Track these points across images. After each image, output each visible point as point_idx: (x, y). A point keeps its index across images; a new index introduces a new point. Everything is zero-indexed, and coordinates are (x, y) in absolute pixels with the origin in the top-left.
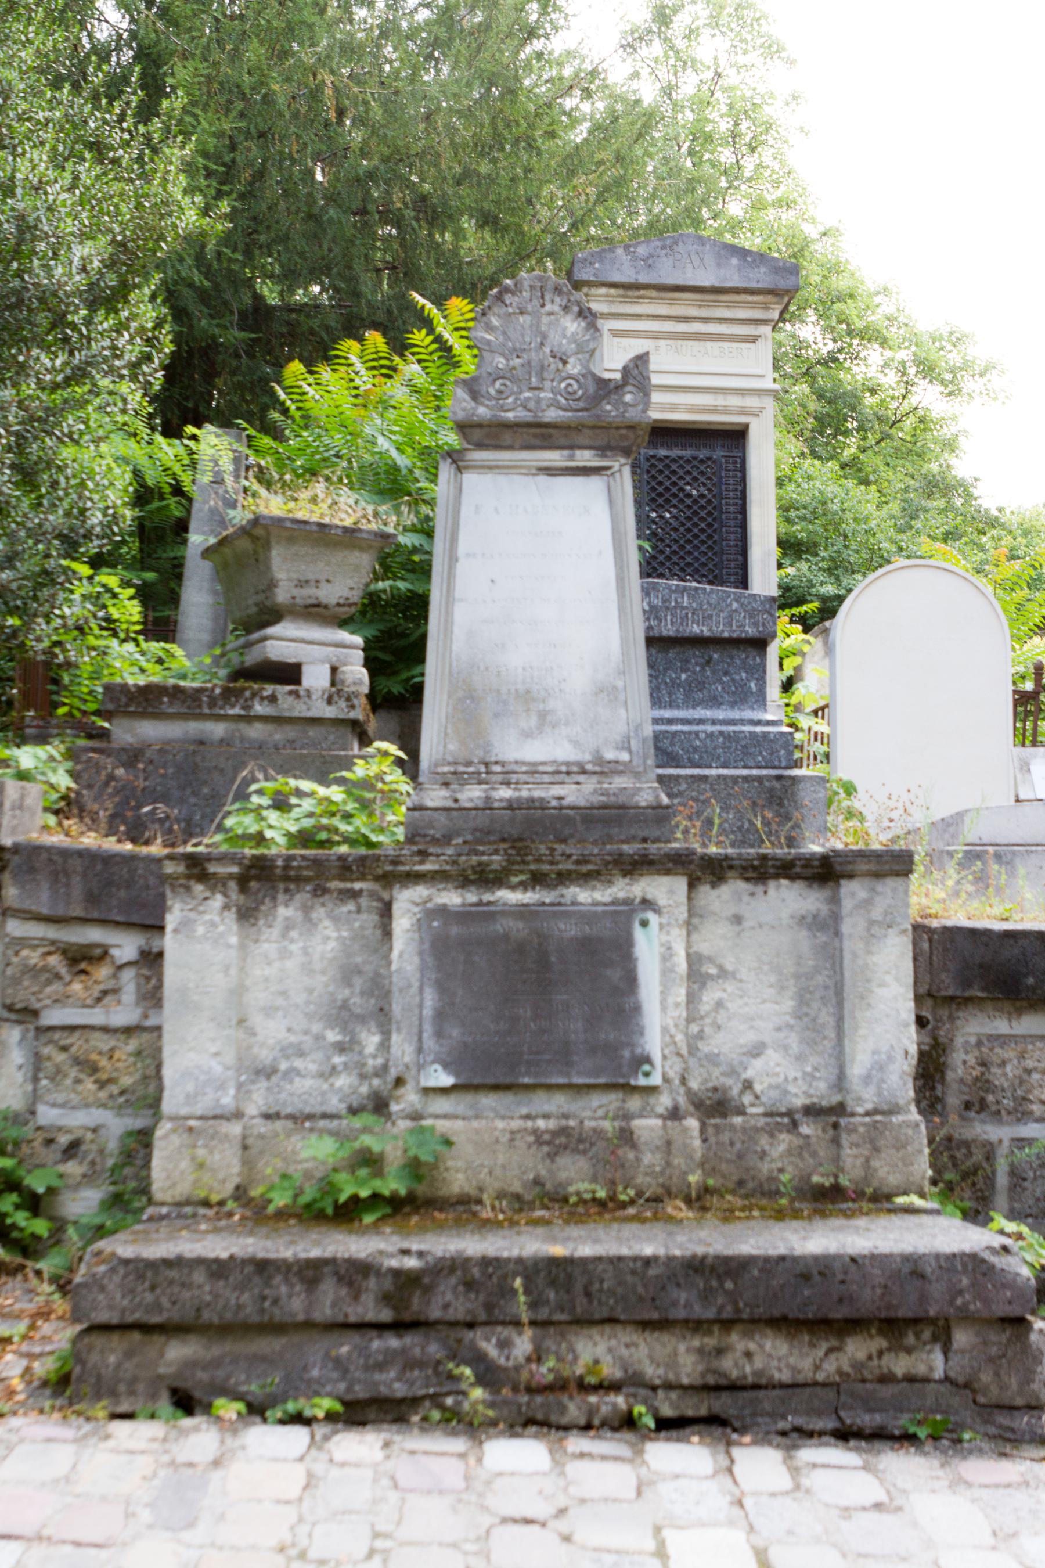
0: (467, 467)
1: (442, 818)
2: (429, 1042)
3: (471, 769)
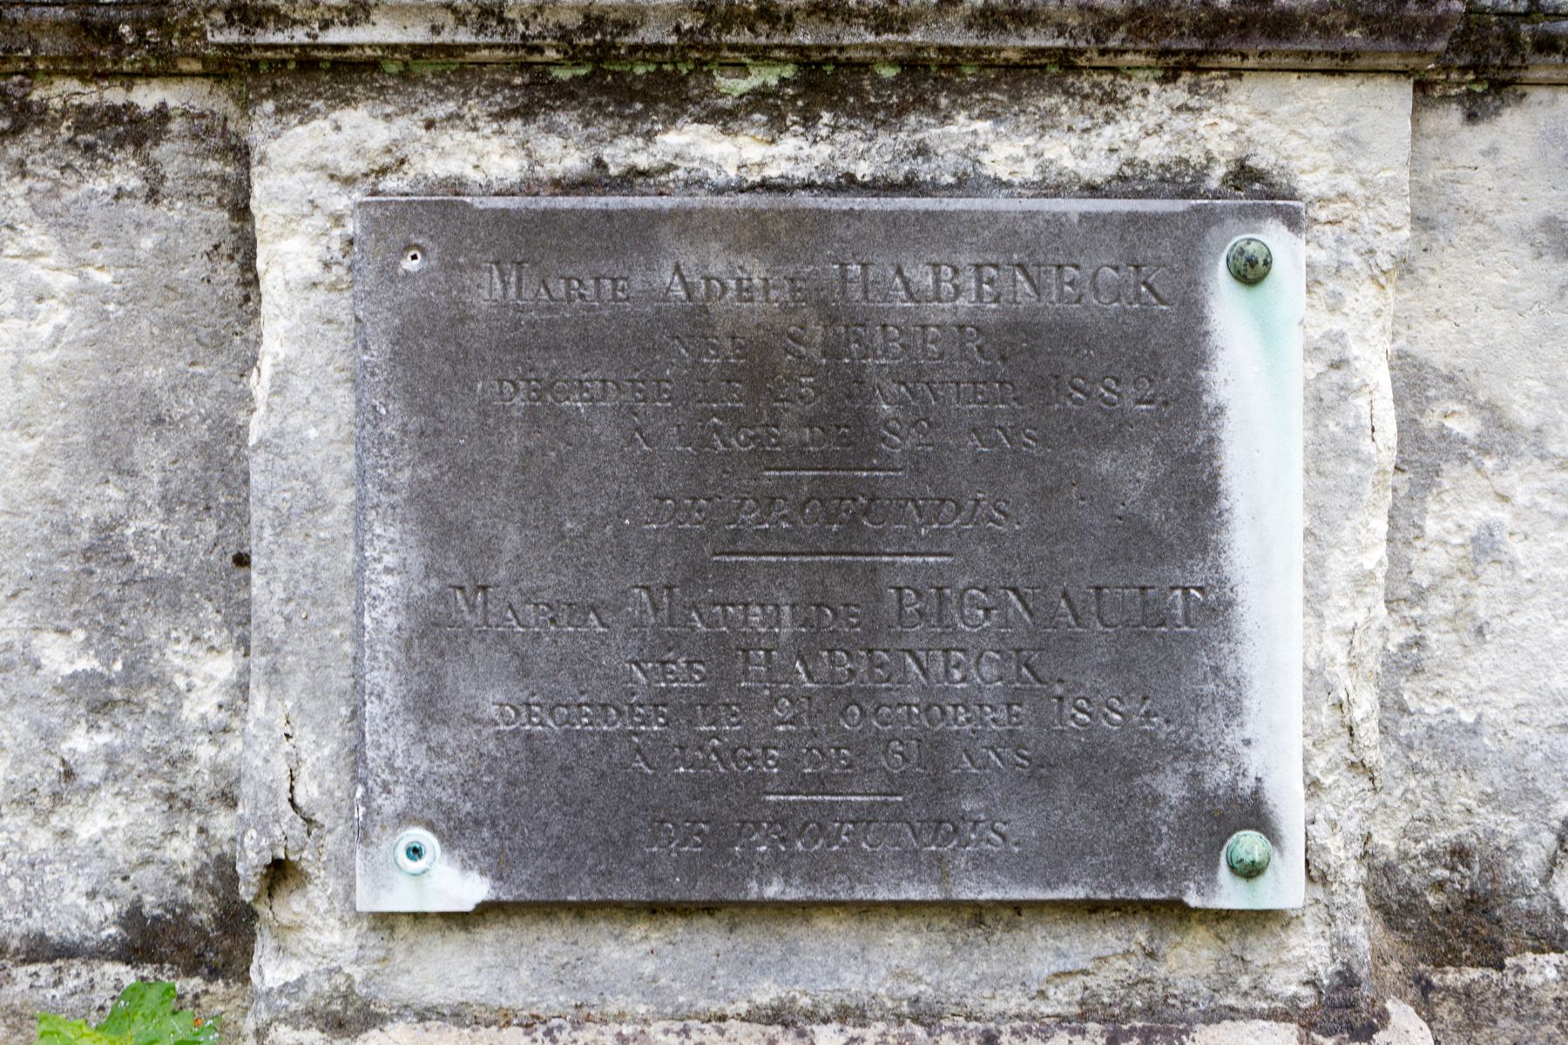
2: (391, 739)
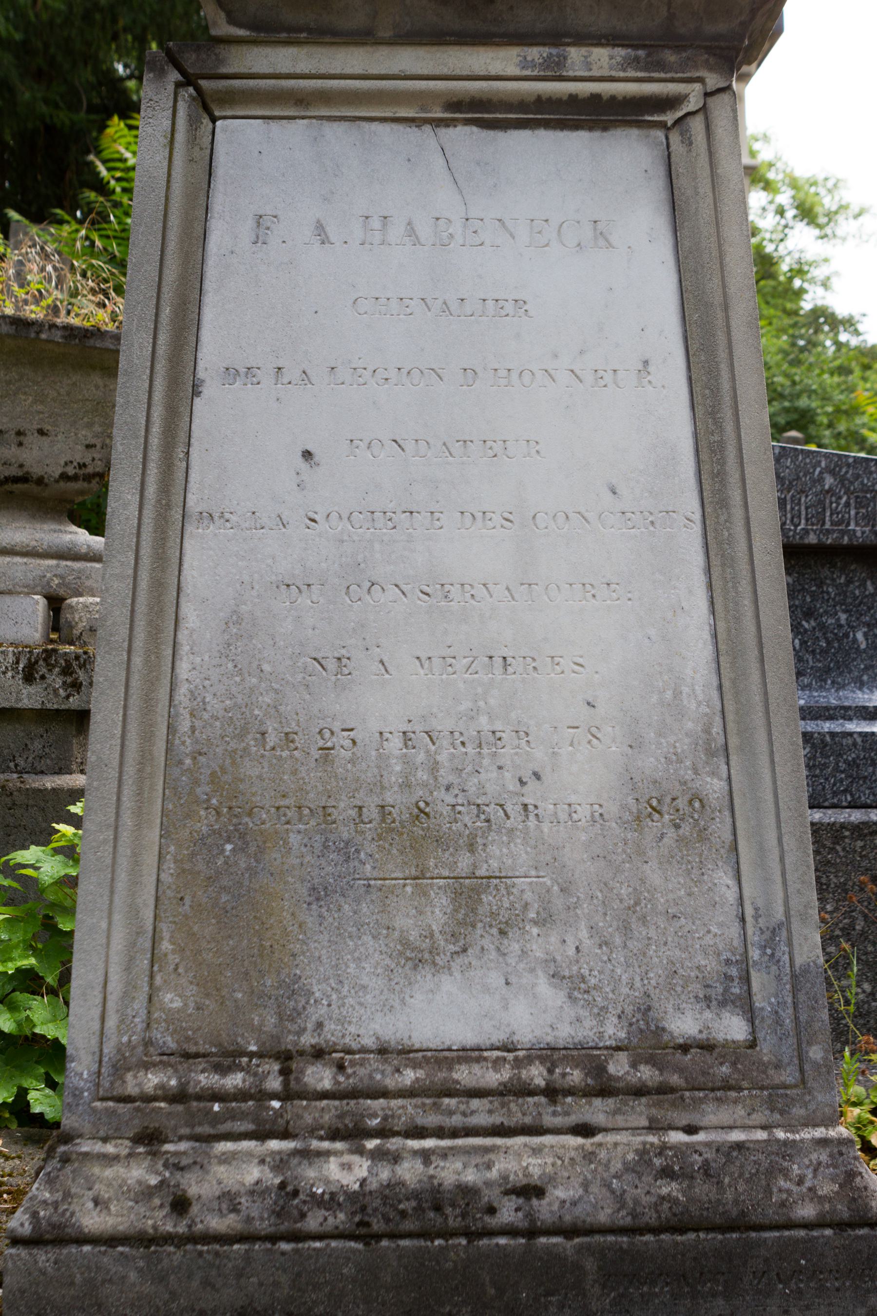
0: (230, 98)
1: (129, 1272)
3: (235, 1080)
